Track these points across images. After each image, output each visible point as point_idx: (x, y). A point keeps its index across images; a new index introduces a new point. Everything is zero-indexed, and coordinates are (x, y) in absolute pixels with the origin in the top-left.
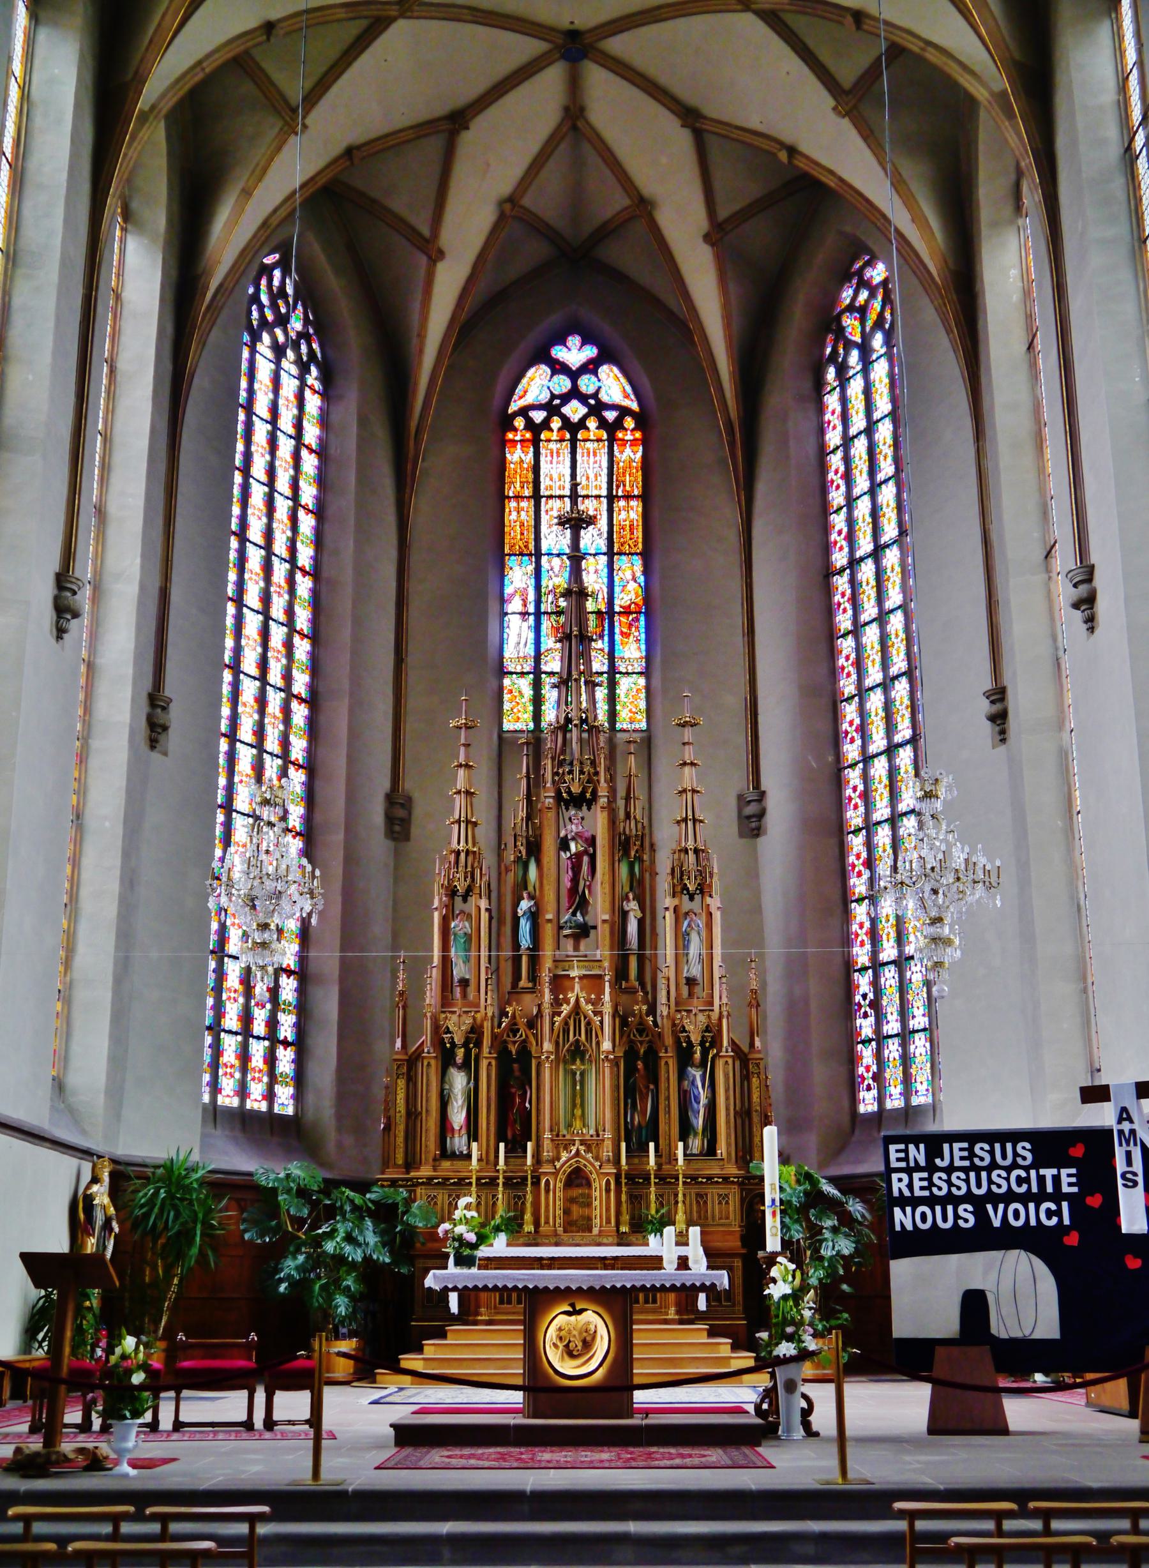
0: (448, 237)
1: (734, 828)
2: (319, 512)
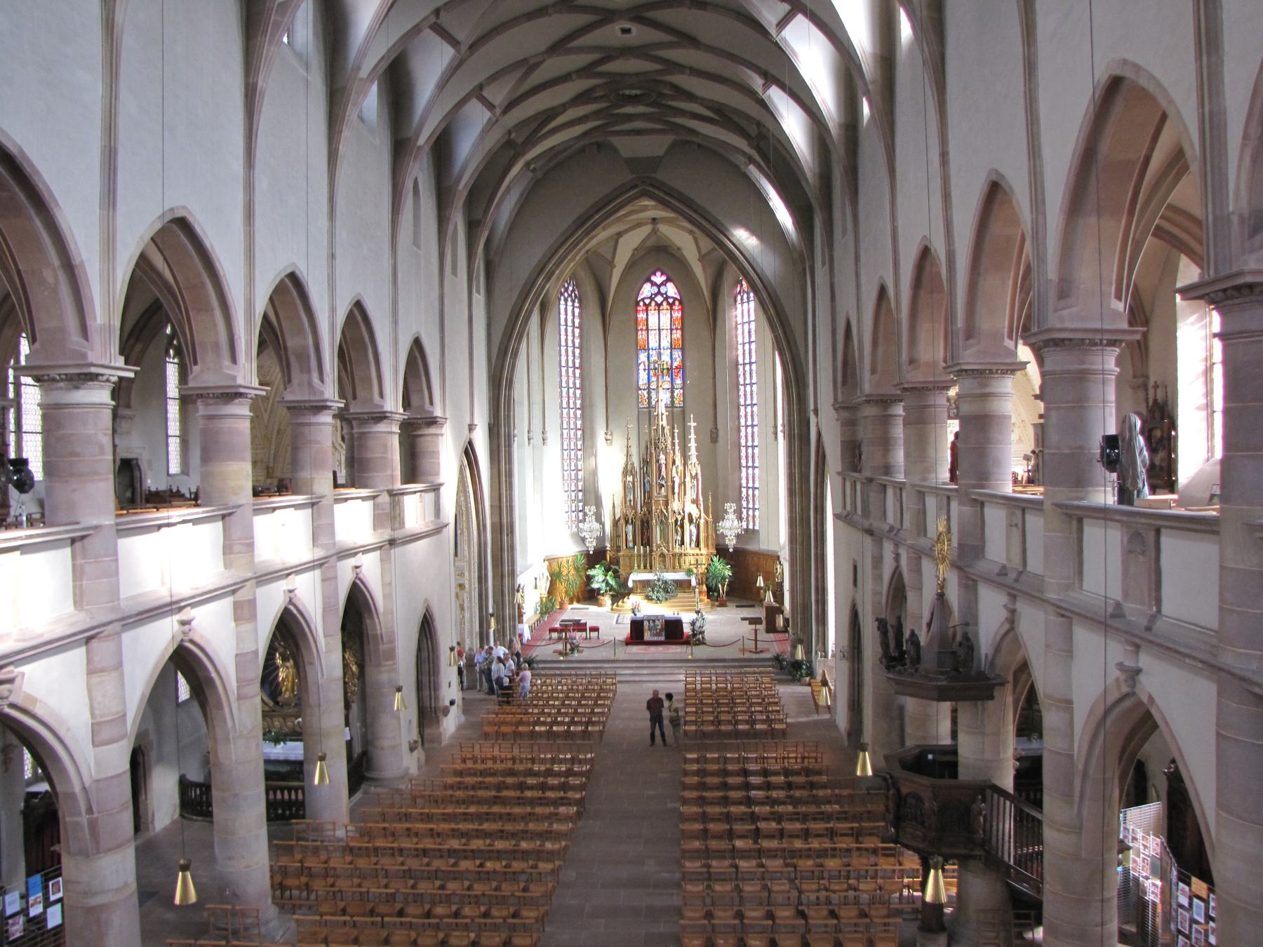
2: (581, 348)
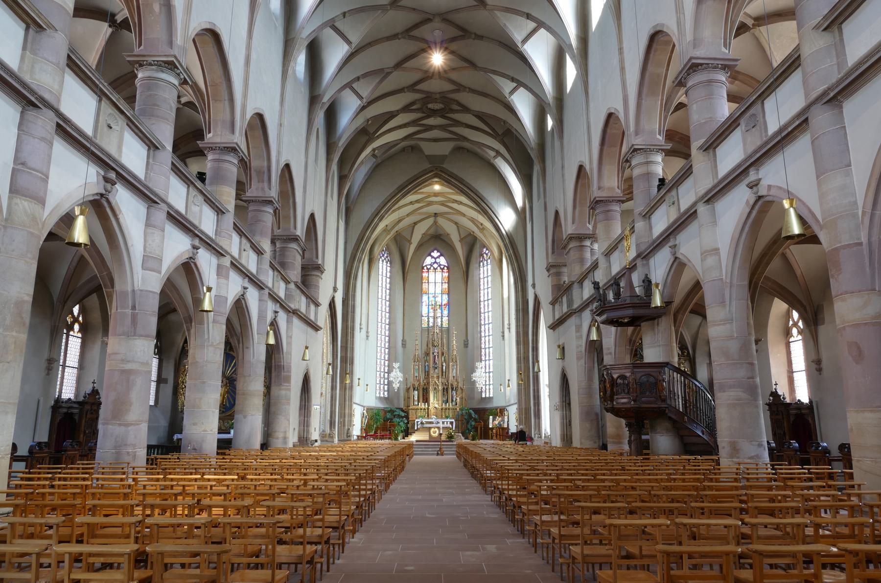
0: (412, 241)
1: (463, 346)
2: (390, 289)
